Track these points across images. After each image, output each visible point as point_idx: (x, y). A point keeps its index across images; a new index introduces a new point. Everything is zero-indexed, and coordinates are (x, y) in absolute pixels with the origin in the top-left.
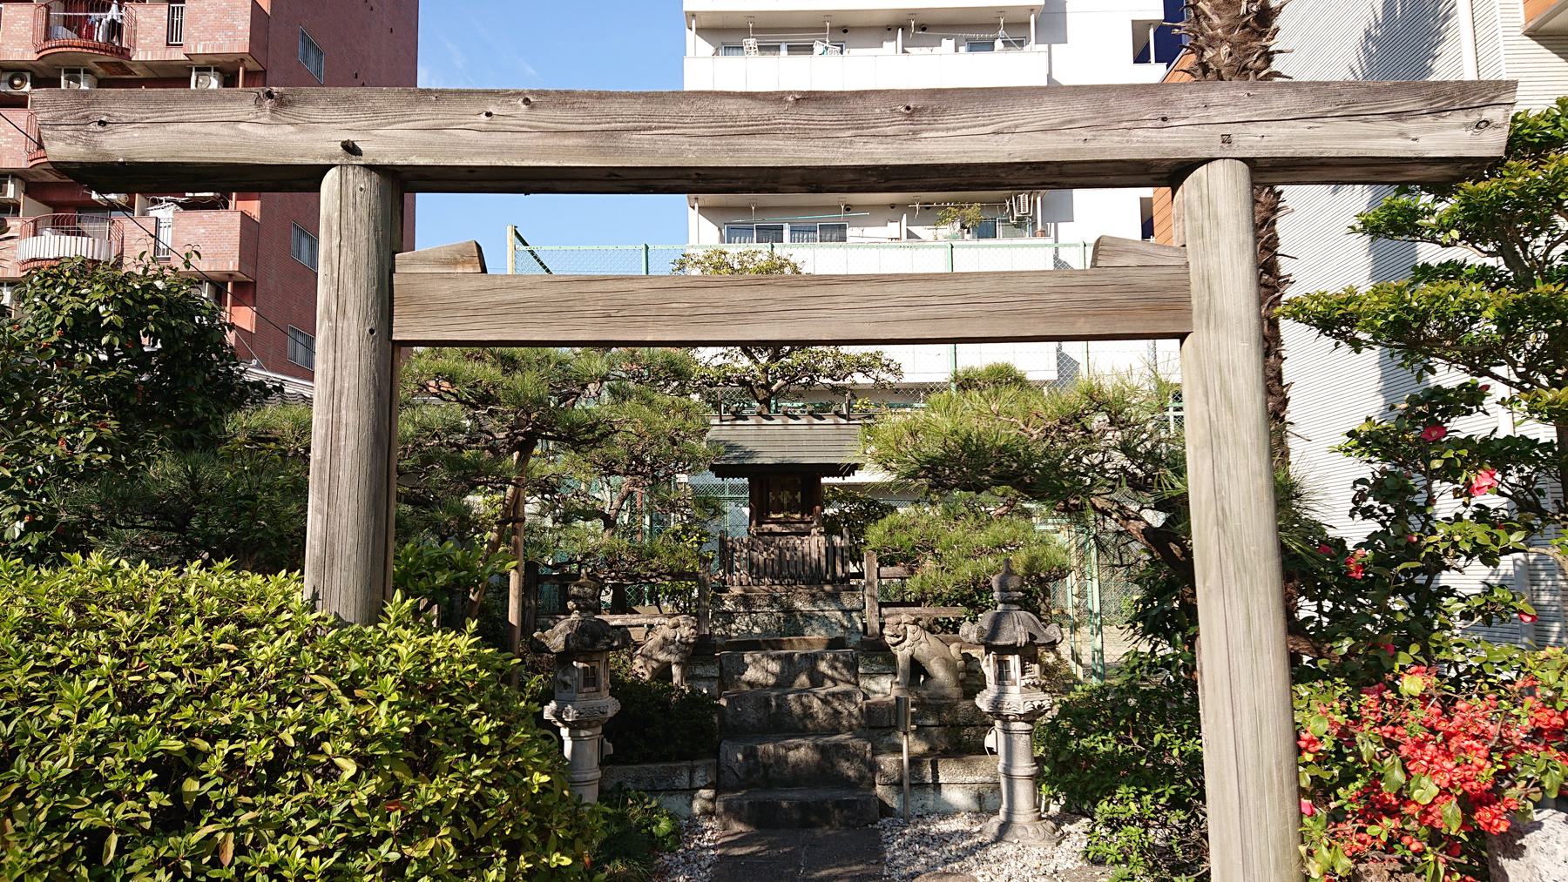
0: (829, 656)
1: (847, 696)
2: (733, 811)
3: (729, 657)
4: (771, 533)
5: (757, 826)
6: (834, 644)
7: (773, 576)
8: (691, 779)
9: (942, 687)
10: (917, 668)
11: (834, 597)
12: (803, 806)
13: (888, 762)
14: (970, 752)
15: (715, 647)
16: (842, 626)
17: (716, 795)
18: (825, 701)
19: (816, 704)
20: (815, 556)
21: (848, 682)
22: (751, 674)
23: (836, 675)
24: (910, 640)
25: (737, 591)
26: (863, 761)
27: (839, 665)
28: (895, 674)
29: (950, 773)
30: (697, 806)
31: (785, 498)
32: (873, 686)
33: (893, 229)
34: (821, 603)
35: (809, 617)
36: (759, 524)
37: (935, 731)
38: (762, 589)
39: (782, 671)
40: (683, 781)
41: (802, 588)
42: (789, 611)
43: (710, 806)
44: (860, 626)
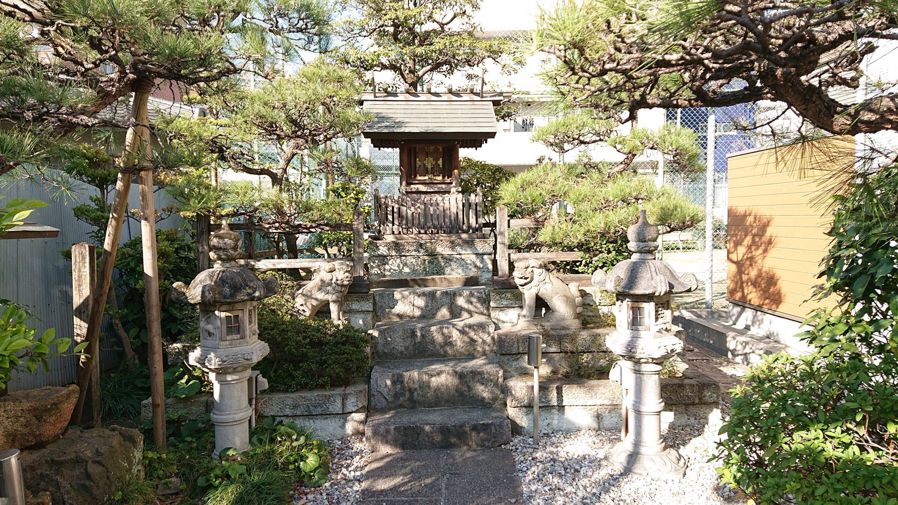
0: (466, 293)
1: (482, 327)
2: (381, 435)
3: (381, 295)
5: (403, 446)
6: (470, 282)
7: (420, 226)
8: (343, 404)
9: (563, 319)
10: (540, 303)
11: (470, 243)
12: (445, 431)
13: (519, 387)
14: (589, 377)
15: (370, 285)
16: (476, 266)
17: (367, 417)
18: (463, 332)
19: (455, 335)
20: (454, 210)
21: (482, 314)
22: (400, 308)
23: (471, 308)
24: (536, 279)
25: (389, 238)
26: (496, 384)
27: (474, 300)
28: (521, 307)
29: (573, 395)
30: (350, 428)
31: (429, 163)
34: (458, 249)
35: (449, 260)
36: (408, 184)
37: (557, 357)
38: (410, 237)
39: (427, 306)
40: (337, 407)
41: (443, 237)
42: (433, 255)
43: (361, 427)
44: (490, 267)
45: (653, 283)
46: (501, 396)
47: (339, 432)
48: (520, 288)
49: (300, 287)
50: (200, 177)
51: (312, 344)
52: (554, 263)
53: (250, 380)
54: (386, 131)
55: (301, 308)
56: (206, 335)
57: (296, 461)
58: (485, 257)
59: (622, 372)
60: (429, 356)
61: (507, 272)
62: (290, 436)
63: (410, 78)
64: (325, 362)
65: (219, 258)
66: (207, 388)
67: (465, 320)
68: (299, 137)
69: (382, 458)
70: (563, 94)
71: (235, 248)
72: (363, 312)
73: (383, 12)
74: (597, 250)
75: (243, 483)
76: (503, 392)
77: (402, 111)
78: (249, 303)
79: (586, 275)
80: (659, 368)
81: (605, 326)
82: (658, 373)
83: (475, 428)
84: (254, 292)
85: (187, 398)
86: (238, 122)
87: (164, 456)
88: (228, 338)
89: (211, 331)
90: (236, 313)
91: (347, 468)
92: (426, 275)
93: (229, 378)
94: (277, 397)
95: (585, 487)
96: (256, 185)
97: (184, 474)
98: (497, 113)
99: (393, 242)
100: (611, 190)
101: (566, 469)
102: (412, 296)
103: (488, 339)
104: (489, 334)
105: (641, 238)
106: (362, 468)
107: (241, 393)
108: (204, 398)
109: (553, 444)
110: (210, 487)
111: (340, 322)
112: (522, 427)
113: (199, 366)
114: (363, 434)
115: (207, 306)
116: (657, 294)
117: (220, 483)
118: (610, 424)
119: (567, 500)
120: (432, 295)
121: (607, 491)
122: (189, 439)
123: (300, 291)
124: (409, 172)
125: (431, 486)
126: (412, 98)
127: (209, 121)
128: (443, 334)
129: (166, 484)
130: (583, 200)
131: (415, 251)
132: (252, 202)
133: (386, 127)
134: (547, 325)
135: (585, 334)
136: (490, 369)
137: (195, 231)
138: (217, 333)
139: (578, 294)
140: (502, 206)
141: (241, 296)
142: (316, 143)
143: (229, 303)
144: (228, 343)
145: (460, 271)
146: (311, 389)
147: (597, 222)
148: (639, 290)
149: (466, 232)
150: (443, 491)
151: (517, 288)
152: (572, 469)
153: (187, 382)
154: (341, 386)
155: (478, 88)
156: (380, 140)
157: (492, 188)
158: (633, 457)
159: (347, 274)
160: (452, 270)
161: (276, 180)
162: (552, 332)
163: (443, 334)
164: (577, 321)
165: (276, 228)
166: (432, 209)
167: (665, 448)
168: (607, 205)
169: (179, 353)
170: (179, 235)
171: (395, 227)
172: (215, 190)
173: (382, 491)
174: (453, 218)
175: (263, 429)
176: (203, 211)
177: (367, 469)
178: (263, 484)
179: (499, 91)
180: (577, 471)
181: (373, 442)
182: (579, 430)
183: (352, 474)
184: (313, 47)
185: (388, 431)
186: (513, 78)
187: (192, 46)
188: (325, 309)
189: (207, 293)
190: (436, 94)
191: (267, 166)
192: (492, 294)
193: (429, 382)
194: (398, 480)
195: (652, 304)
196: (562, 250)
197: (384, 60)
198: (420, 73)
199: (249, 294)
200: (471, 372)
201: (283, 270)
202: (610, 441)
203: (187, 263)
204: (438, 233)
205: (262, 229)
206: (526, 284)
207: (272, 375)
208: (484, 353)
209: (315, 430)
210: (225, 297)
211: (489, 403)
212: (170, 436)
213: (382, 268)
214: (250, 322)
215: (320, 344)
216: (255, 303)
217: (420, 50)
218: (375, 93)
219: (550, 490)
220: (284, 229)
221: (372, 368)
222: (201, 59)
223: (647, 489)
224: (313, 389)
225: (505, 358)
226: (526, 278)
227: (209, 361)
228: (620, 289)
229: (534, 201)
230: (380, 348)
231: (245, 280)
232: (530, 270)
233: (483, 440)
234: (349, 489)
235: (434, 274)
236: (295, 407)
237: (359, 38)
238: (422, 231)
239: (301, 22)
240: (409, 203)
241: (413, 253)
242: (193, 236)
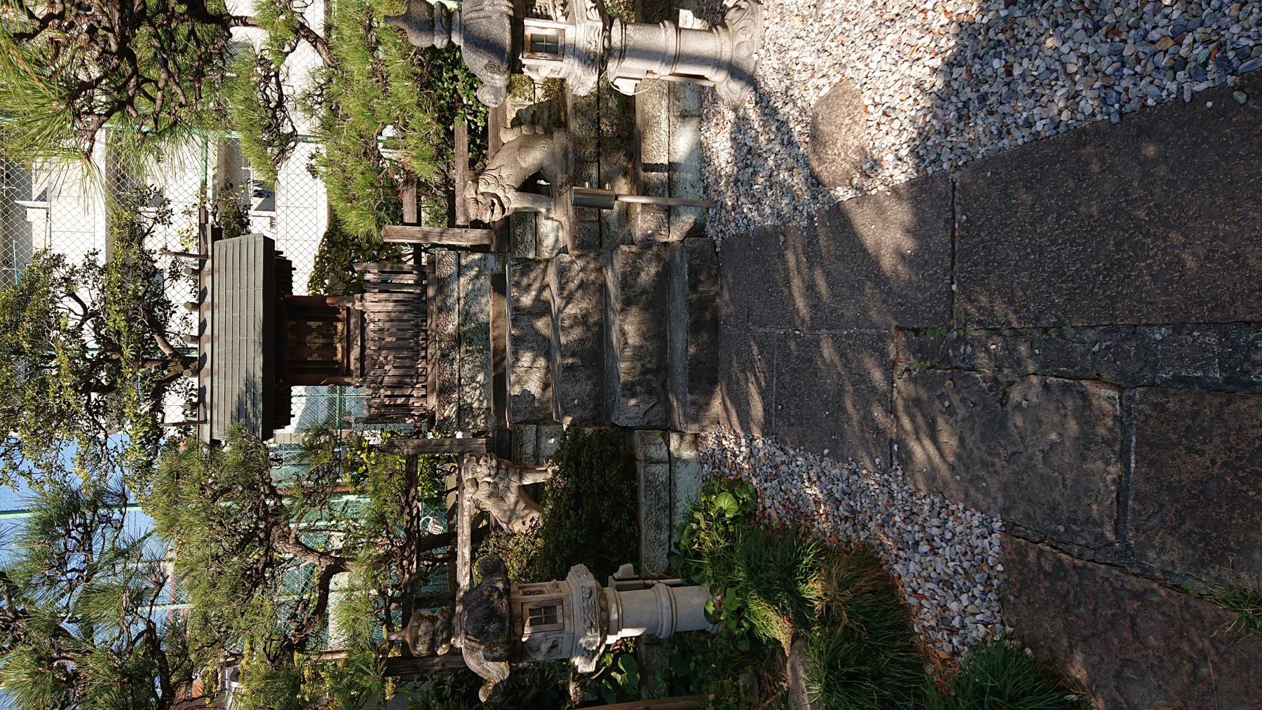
0: (514, 292)
1: (562, 272)
2: (698, 412)
3: (514, 413)
4: (362, 358)
5: (714, 383)
6: (499, 286)
7: (415, 357)
8: (658, 462)
9: (552, 155)
10: (528, 185)
11: (442, 284)
12: (695, 328)
13: (643, 224)
14: (631, 124)
15: (500, 429)
16: (477, 277)
17: (675, 431)
18: (569, 299)
19: (572, 310)
20: (390, 306)
21: (545, 271)
22: (534, 387)
23: (536, 286)
24: (495, 190)
25: (432, 402)
26: (639, 255)
27: (525, 281)
28: (536, 214)
30: (688, 453)
31: (315, 341)
32: (549, 242)
34: (450, 301)
35: (466, 316)
36: (349, 373)
37: (605, 168)
38: (432, 372)
39: (532, 349)
40: (660, 471)
41: (431, 323)
43: (688, 438)
44: (477, 256)
45: (495, 17)
46: (655, 249)
47: (693, 468)
48: (507, 213)
49: (498, 527)
50: (333, 677)
51: (578, 506)
52: (472, 163)
53: (619, 589)
54: (260, 406)
55: (528, 523)
56: (555, 651)
57: (724, 523)
58: (463, 262)
59: (627, 77)
60: (601, 346)
61: (485, 231)
62: (693, 532)
63: (175, 367)
64: (602, 488)
65: (447, 640)
66: (630, 644)
67: (552, 294)
68: (268, 535)
69: (727, 410)
70: (175, 123)
71: (433, 620)
72: (538, 438)
73: (64, 407)
74: (452, 97)
75: (748, 591)
76: (649, 247)
77: (229, 381)
78: (513, 596)
79: (489, 116)
80: (617, 22)
81: (564, 96)
82: (624, 24)
83: (693, 287)
84: (497, 589)
85: (642, 670)
86: (242, 625)
87: (711, 697)
88: (560, 621)
89: (549, 645)
90: (526, 612)
91: (736, 456)
92: (488, 349)
93: (614, 616)
94: (644, 552)
95: (770, 141)
96: (342, 596)
97: (735, 670)
98: (234, 233)
99: (438, 397)
100: (357, 67)
101: (747, 166)
102: (518, 370)
103: (580, 264)
104: (572, 262)
105: (428, 27)
106: (737, 436)
107: (637, 600)
108: (643, 648)
109: (717, 182)
110: (751, 634)
111: (550, 470)
112: (695, 223)
113: (596, 659)
114: (696, 436)
115: (515, 652)
116: (511, 13)
117: (747, 621)
118: (693, 102)
119: (783, 166)
120: (516, 341)
121: (775, 110)
122: (692, 665)
123: (504, 526)
124: (329, 372)
125: (762, 347)
126: (208, 365)
127: (247, 668)
128: (571, 327)
129: (745, 692)
130: (372, 110)
131: (452, 364)
132: (367, 600)
133: (254, 405)
134: (561, 178)
135: (574, 125)
136: (619, 262)
137: (416, 677)
138: (552, 637)
139: (516, 130)
140: (382, 233)
141: (502, 606)
142: (279, 510)
143: (512, 623)
144: (567, 621)
145: (484, 300)
146: (637, 506)
147: (404, 90)
148: (506, 38)
149: (425, 288)
150: (767, 330)
151: (507, 218)
152: (746, 155)
153: (621, 672)
154: (635, 466)
155: (193, 263)
156: (278, 414)
157: (359, 248)
158: (735, 71)
159: (481, 462)
160: (482, 311)
161: (337, 566)
162: (571, 172)
163: (571, 327)
164: (556, 135)
165: (411, 563)
166: (389, 339)
167: (725, 26)
168: (380, 76)
169: (582, 686)
170: (419, 697)
171: (415, 393)
172: (350, 652)
173: (765, 410)
174: (403, 308)
175: (684, 569)
176: (379, 668)
177: (738, 431)
178: (748, 564)
179: (197, 230)
180: (749, 151)
181: (706, 422)
182: (700, 144)
183: (743, 449)
184: (116, 515)
185: (694, 403)
186: (177, 208)
187: (106, 696)
188: (531, 491)
189: (496, 654)
190: (202, 326)
191: (316, 581)
192: (517, 255)
193: (635, 347)
194: (753, 389)
195: (526, 22)
196: (453, 148)
197: (145, 408)
198: (167, 352)
199: (500, 597)
200: (623, 289)
201: (473, 552)
202: (715, 102)
203: (461, 686)
204: (426, 331)
205: (411, 583)
206: (502, 205)
207: (616, 559)
208: (599, 270)
209: (688, 499)
210: (502, 630)
211: (664, 267)
212: (688, 690)
213: (476, 413)
214: (541, 592)
215: (577, 496)
216: (514, 588)
217: (128, 353)
218: (199, 422)
219: (771, 188)
220: (412, 552)
221: (613, 425)
222: (130, 681)
223: (773, 57)
224: (637, 504)
225: (606, 241)
226: (493, 204)
227: (591, 644)
228: (504, 67)
229: (372, 185)
230: (587, 414)
231: (479, 604)
232: (480, 198)
233: (709, 276)
234: (761, 454)
235: (488, 338)
236: (658, 526)
237: (110, 445)
238: (423, 354)
239: (73, 533)
240: (379, 372)
241: (456, 367)
242: (424, 679)
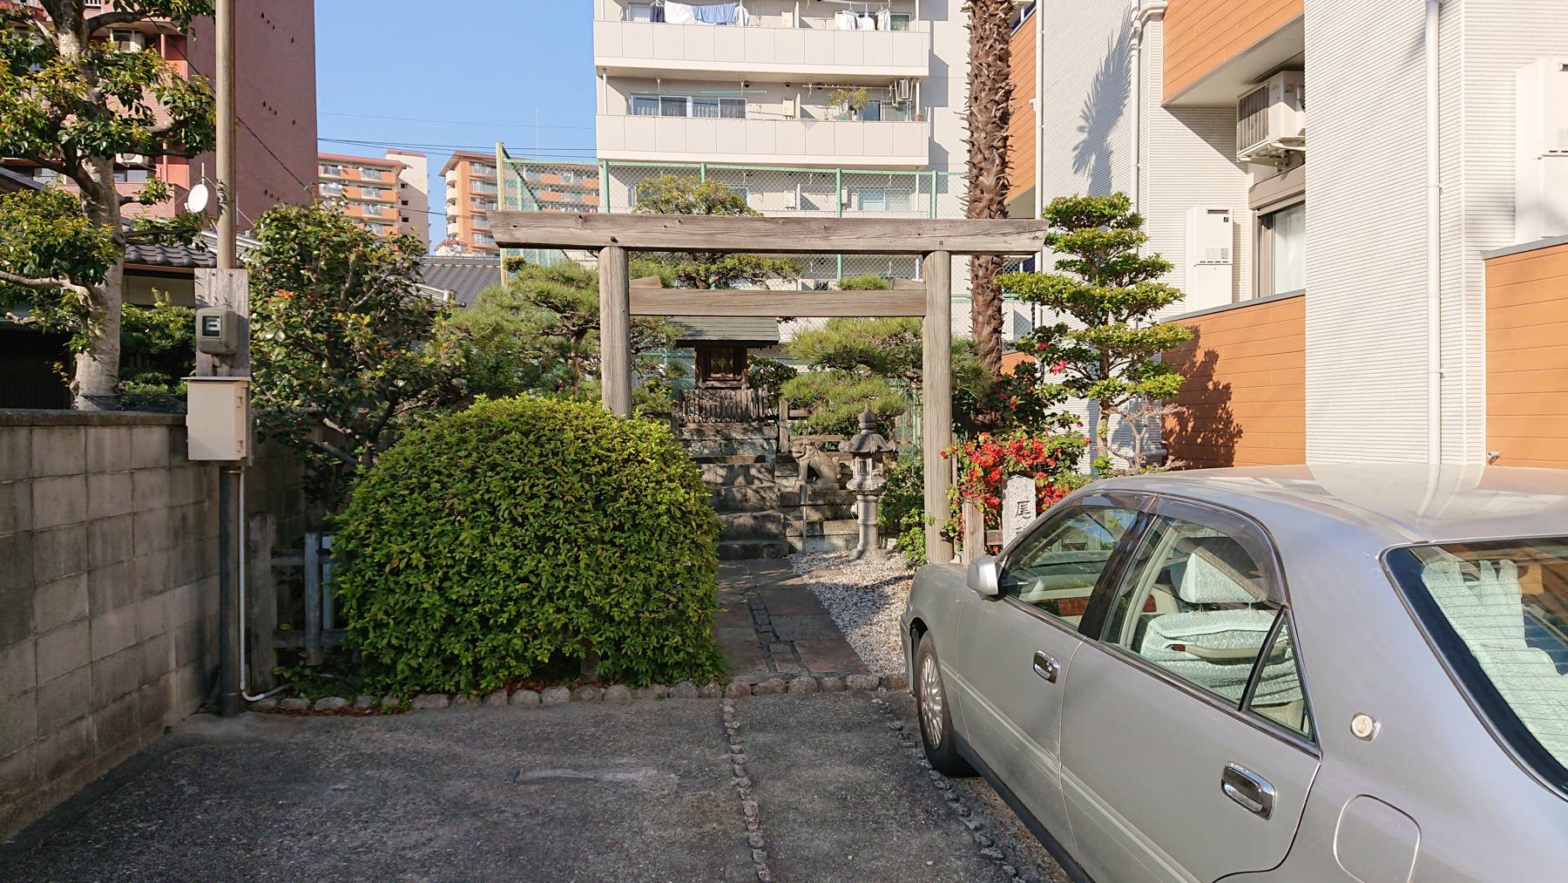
4: (713, 388)
6: (760, 459)
11: (759, 430)
32: (784, 482)
33: (788, 107)
35: (741, 443)
42: (728, 439)
